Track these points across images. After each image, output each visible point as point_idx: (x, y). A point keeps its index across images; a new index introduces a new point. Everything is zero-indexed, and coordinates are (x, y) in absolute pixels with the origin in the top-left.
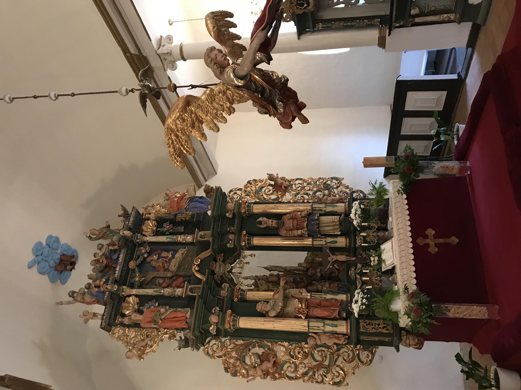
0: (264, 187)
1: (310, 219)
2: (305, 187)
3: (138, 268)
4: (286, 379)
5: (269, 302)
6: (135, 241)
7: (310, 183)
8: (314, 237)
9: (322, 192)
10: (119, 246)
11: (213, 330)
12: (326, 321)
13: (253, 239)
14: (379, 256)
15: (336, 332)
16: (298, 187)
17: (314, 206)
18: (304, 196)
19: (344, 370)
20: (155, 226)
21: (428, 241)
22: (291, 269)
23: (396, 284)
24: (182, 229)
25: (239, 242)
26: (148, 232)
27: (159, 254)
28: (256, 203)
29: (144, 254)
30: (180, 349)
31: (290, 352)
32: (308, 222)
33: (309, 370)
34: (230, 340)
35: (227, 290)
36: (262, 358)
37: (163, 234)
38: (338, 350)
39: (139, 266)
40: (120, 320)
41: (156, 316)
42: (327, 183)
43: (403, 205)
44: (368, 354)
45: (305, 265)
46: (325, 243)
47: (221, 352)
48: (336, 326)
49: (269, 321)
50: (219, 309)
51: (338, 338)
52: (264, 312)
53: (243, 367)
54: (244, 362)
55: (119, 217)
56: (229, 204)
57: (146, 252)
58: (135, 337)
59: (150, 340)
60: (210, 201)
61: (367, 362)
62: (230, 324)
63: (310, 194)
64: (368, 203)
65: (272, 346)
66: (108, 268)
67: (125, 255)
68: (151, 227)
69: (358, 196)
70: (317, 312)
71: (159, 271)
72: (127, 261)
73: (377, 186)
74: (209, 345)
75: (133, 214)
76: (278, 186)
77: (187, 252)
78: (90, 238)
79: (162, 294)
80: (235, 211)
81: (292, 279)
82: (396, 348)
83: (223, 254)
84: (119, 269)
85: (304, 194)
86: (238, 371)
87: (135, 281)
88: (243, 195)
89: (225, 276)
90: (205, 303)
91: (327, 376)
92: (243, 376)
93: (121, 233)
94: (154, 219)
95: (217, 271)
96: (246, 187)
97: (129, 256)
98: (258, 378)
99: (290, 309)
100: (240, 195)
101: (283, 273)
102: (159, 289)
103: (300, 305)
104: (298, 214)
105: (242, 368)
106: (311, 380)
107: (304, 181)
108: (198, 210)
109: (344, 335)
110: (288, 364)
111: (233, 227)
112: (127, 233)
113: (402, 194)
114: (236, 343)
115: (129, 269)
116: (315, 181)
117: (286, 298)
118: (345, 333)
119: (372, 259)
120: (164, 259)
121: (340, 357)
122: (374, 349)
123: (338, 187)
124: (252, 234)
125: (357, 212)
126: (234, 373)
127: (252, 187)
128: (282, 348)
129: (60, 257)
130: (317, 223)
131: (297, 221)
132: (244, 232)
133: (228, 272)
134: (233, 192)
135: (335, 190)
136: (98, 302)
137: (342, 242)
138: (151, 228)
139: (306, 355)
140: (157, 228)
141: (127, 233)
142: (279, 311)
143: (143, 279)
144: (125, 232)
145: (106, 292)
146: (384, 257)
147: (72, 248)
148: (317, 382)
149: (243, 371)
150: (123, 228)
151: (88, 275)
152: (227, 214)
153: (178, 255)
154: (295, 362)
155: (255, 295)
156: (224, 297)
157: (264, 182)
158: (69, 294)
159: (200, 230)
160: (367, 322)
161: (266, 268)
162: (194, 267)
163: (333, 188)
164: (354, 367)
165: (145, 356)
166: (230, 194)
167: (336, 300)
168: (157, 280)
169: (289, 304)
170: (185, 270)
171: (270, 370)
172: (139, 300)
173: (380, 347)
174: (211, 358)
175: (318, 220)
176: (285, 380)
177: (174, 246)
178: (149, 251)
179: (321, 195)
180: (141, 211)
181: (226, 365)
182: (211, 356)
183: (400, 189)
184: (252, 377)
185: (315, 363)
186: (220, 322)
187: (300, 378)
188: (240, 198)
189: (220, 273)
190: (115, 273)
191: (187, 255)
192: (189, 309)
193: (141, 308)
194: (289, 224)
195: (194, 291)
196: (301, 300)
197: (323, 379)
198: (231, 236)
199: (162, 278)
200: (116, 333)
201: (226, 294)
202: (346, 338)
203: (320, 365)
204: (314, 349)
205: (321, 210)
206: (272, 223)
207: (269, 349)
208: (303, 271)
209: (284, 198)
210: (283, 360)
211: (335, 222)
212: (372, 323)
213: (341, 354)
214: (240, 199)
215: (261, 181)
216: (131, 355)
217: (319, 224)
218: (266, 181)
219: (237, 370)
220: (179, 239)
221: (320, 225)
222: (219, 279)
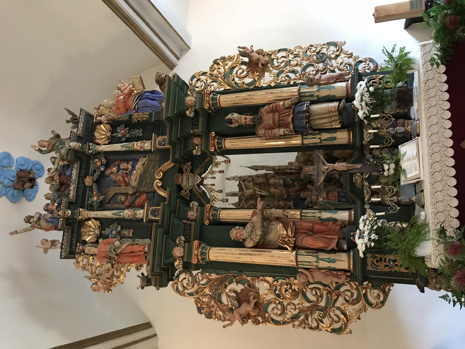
0: (236, 67)
1: (296, 110)
2: (290, 61)
3: (96, 184)
4: (271, 324)
5: (246, 227)
6: (87, 153)
7: (298, 54)
8: (304, 134)
9: (315, 66)
10: (67, 161)
11: (178, 266)
12: (320, 253)
13: (224, 141)
14: (397, 163)
15: (335, 268)
16: (282, 63)
17: (302, 91)
19: (346, 314)
20: (110, 131)
22: (280, 168)
23: (423, 207)
24: (139, 132)
25: (207, 147)
26: (103, 138)
27: (119, 166)
28: (225, 92)
29: (99, 167)
30: (143, 288)
31: (275, 290)
32: (293, 115)
33: (300, 313)
34: (202, 273)
35: (196, 210)
37: (118, 141)
38: (338, 288)
39: (98, 182)
40: (81, 248)
41: (110, 251)
42: (321, 52)
43: (438, 84)
44: (378, 295)
45: (297, 165)
46: (319, 141)
47: (192, 288)
48: (334, 261)
49: (245, 254)
50: (184, 239)
51: (337, 276)
52: (241, 240)
53: (219, 308)
55: (67, 123)
56: (187, 98)
57: (102, 164)
58: (100, 266)
59: (117, 271)
61: (377, 304)
62: (198, 258)
63: (298, 72)
64: (380, 79)
65: (252, 281)
66: (63, 186)
67: (78, 170)
68: (104, 131)
69: (367, 68)
70: (308, 241)
71: (120, 186)
72: (81, 178)
73: (396, 54)
74: (178, 279)
75: (82, 118)
76: (254, 63)
77: (148, 162)
78: (40, 151)
79: (122, 217)
80: (197, 107)
81: (281, 181)
82: (419, 288)
83: (190, 162)
84: (74, 189)
85: (290, 72)
86: (213, 313)
87: (92, 202)
88: (209, 81)
89: (195, 189)
90: (166, 233)
91: (324, 320)
92: (220, 319)
93: (67, 146)
94: (106, 122)
95: (184, 184)
97: (84, 170)
98: (237, 323)
99: (272, 237)
100: (204, 82)
101: (272, 172)
102: (117, 211)
103: (285, 232)
104: (279, 105)
105: (218, 308)
106: (303, 325)
107: (289, 52)
108: (151, 110)
110: (273, 305)
111: (197, 128)
113: (438, 65)
114: (209, 277)
115: (85, 187)
116: (305, 50)
117: (266, 220)
118: (346, 267)
119: (386, 167)
120: (125, 171)
121: (340, 298)
122: (388, 287)
123: (337, 56)
124: (223, 135)
125: (364, 98)
126: (208, 314)
127: (219, 68)
128: (265, 284)
129: (17, 174)
130: (306, 116)
131: (279, 115)
133: (198, 185)
134: (196, 79)
135: (333, 61)
136: (56, 228)
138: (104, 133)
139: (295, 294)
140: (112, 133)
142: (257, 241)
143: (101, 198)
144: (71, 144)
145: (59, 218)
146: (404, 165)
147: (33, 160)
148: (311, 328)
149: (220, 312)
150: (70, 138)
151: (45, 195)
152: (188, 113)
153: (138, 167)
154: (282, 302)
155: (230, 216)
156: (191, 221)
157: (235, 59)
158: (24, 220)
159: (158, 135)
160: (377, 257)
161: (251, 168)
162: (155, 182)
163: (331, 59)
164: (359, 310)
165: (113, 288)
166: (192, 81)
167: (335, 220)
169: (272, 229)
170: (147, 185)
171: (251, 313)
172: (101, 223)
173: (395, 285)
174: (181, 295)
175: (308, 111)
176: (270, 324)
178: (106, 163)
179: (313, 71)
180: (93, 112)
181: (199, 305)
182: (181, 293)
183: (435, 57)
184: (229, 322)
185: (307, 305)
186: (186, 256)
187: (288, 323)
188: (205, 86)
189: (188, 187)
190: (69, 194)
191: (148, 165)
192: (148, 241)
193: (103, 232)
194: (268, 119)
195: (156, 213)
196: (287, 224)
197: (318, 324)
198: (197, 141)
199: (124, 194)
200: (80, 261)
201: (195, 215)
202: (348, 276)
203: (314, 307)
204: (306, 286)
205: (312, 96)
206: (245, 119)
207: (248, 285)
208: (295, 170)
209: (262, 81)
210: (267, 300)
211: (332, 112)
212: (385, 259)
213: (342, 294)
214: (205, 88)
215: (231, 58)
216: (97, 288)
217: (309, 116)
218: (237, 58)
219: (212, 311)
220: (135, 147)
221: (312, 118)
222: (187, 195)
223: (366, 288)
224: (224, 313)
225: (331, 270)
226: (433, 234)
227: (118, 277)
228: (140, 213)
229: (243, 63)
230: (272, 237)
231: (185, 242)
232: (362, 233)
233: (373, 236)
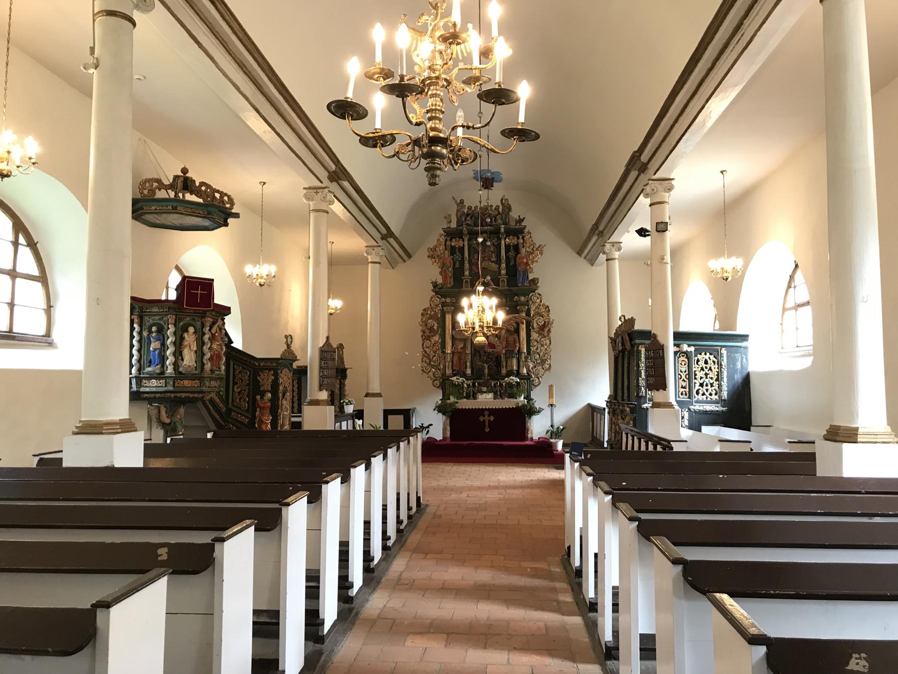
18: (536, 347)
21: (487, 416)
36: (431, 329)
37: (506, 253)
38: (439, 369)
48: (448, 368)
54: (429, 319)
60: (525, 284)
70: (456, 358)
78: (502, 200)
92: (422, 320)
96: (544, 305)
98: (421, 328)
102: (468, 259)
109: (445, 372)
110: (429, 342)
112: (502, 230)
118: (446, 373)
119: (485, 388)
123: (543, 369)
137: (504, 371)
139: (435, 352)
141: (502, 230)
148: (422, 359)
152: (516, 297)
163: (542, 366)
165: (430, 259)
177: (498, 262)
180: (526, 230)
185: (431, 357)
194: (511, 339)
203: (431, 360)
209: (533, 333)
214: (533, 302)
223: (440, 380)
224: (424, 322)
225: (445, 366)
226: (456, 400)
228: (467, 273)
229: (545, 322)
230: (457, 342)
231: (453, 303)
233: (456, 383)
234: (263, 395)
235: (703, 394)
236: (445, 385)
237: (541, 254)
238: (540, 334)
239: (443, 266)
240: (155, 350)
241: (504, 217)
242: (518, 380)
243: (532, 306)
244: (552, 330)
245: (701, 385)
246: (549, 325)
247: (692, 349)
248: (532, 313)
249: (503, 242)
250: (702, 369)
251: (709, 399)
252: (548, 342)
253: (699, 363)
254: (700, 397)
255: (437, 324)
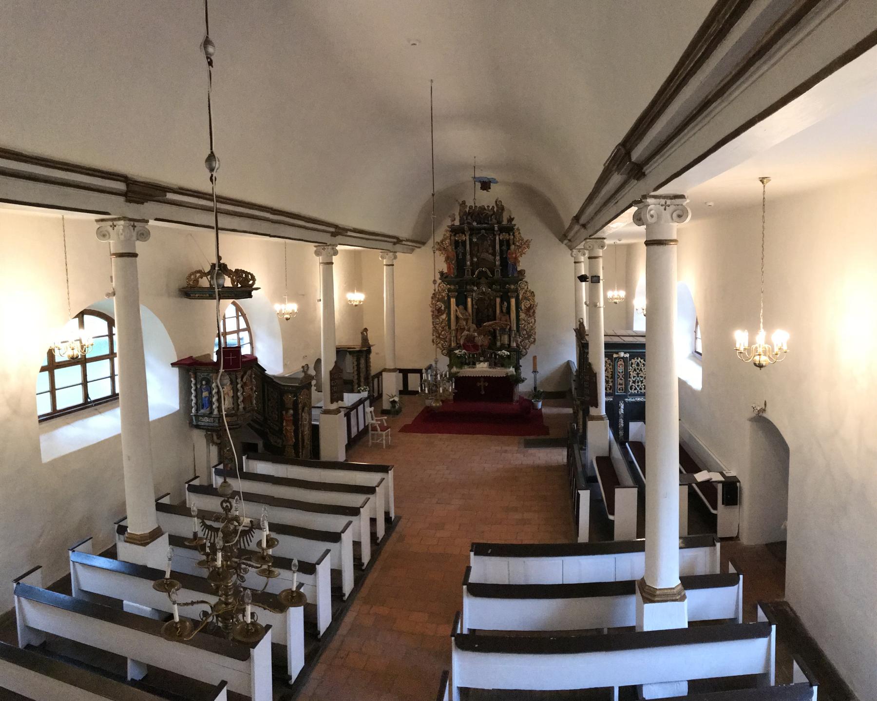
37: (501, 246)
38: (446, 342)
48: (454, 342)
72: (485, 229)
78: (496, 202)
92: (432, 302)
112: (496, 228)
123: (529, 342)
132: (501, 294)
137: (498, 344)
139: (443, 328)
141: (496, 228)
146: (482, 363)
168: (477, 247)
180: (516, 227)
185: (440, 332)
199: (478, 249)
203: (440, 334)
225: (451, 340)
227: (442, 253)
228: (468, 263)
229: (531, 305)
232: (461, 352)
234: (287, 410)
235: (636, 389)
236: (450, 353)
237: (528, 247)
238: (527, 315)
239: (447, 259)
240: (206, 397)
241: (498, 217)
242: (509, 354)
243: (520, 292)
244: (536, 311)
245: (634, 382)
246: (534, 308)
247: (627, 355)
248: (521, 297)
249: (497, 238)
250: (635, 370)
251: (639, 393)
252: (533, 320)
253: (633, 366)
254: (633, 391)
255: (444, 305)
